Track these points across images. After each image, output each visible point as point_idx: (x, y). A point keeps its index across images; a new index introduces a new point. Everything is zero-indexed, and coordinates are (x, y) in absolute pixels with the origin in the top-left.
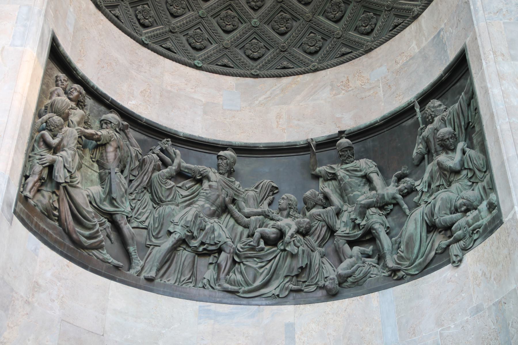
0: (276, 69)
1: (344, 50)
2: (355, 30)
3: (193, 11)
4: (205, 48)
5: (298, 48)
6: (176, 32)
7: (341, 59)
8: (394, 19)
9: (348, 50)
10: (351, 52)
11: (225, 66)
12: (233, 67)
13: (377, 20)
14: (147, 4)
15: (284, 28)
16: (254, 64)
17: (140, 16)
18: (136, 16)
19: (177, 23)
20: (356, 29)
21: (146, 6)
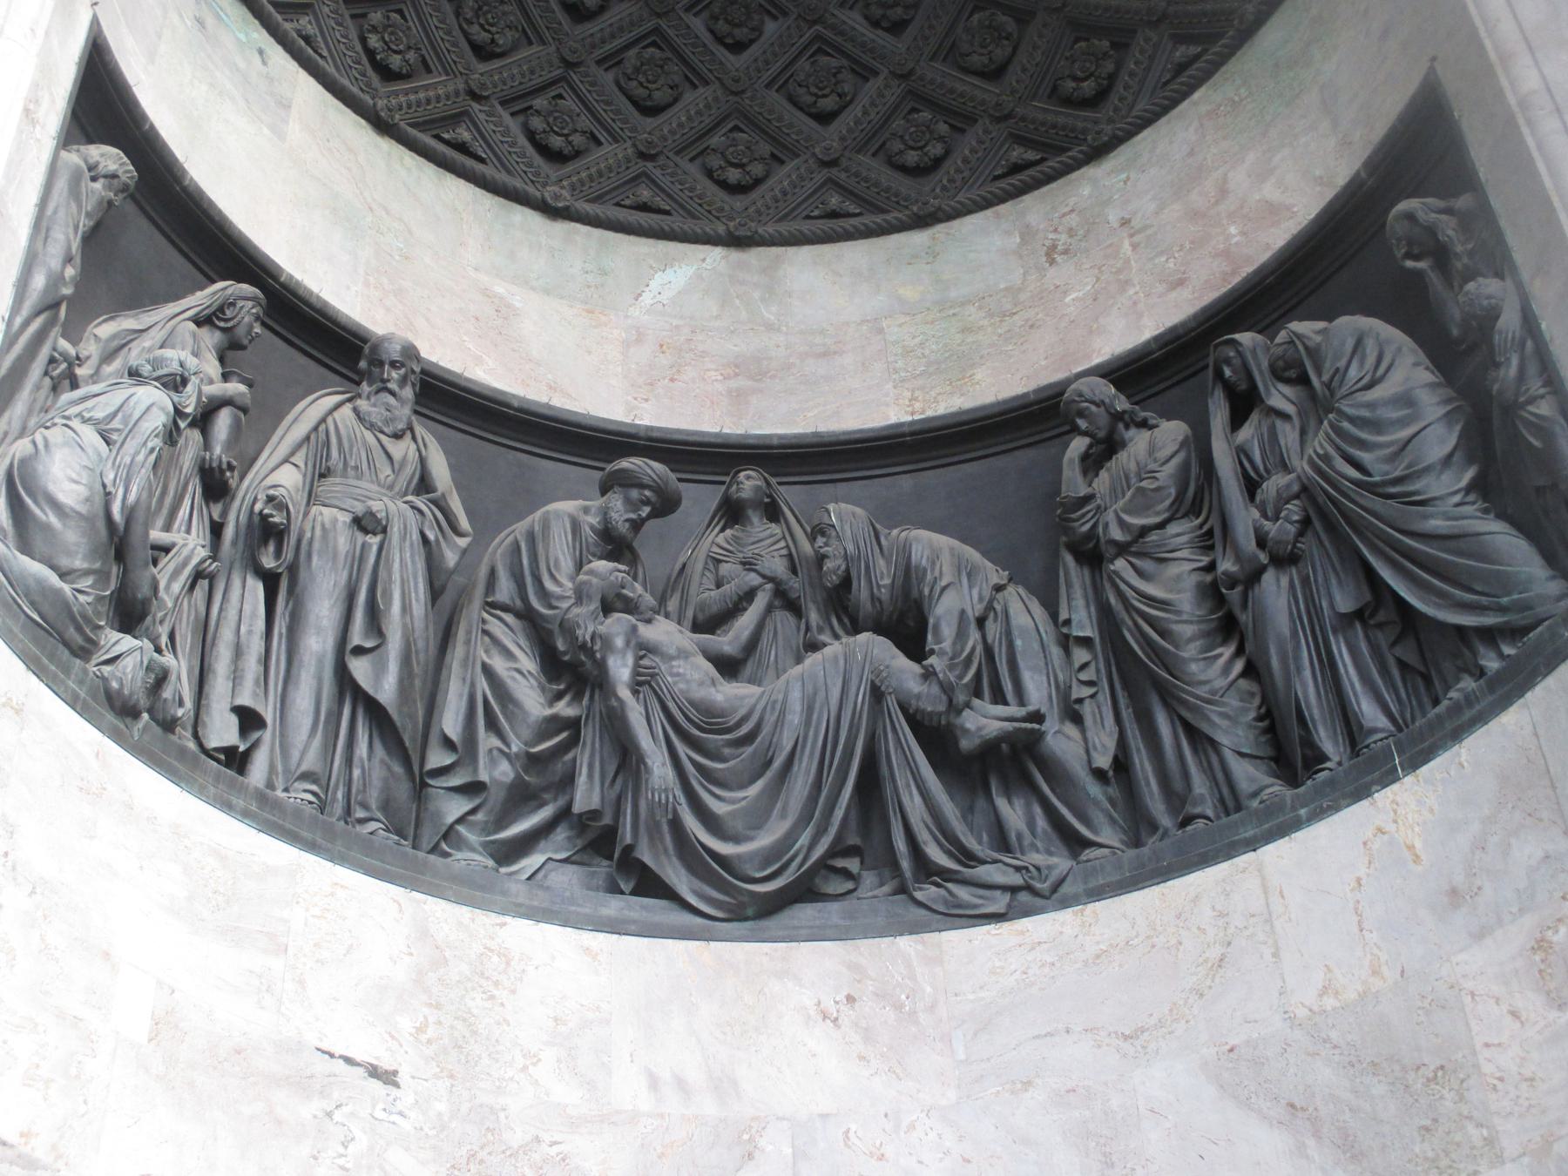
0: (808, 217)
1: (1017, 154)
2: (1049, 97)
3: (544, 43)
4: (577, 154)
5: (874, 155)
6: (486, 98)
7: (1015, 180)
9: (1032, 155)
10: (1043, 160)
12: (667, 213)
13: (1119, 65)
14: (400, 12)
15: (834, 97)
16: (738, 202)
17: (374, 41)
18: (363, 40)
19: (490, 73)
21: (394, 15)
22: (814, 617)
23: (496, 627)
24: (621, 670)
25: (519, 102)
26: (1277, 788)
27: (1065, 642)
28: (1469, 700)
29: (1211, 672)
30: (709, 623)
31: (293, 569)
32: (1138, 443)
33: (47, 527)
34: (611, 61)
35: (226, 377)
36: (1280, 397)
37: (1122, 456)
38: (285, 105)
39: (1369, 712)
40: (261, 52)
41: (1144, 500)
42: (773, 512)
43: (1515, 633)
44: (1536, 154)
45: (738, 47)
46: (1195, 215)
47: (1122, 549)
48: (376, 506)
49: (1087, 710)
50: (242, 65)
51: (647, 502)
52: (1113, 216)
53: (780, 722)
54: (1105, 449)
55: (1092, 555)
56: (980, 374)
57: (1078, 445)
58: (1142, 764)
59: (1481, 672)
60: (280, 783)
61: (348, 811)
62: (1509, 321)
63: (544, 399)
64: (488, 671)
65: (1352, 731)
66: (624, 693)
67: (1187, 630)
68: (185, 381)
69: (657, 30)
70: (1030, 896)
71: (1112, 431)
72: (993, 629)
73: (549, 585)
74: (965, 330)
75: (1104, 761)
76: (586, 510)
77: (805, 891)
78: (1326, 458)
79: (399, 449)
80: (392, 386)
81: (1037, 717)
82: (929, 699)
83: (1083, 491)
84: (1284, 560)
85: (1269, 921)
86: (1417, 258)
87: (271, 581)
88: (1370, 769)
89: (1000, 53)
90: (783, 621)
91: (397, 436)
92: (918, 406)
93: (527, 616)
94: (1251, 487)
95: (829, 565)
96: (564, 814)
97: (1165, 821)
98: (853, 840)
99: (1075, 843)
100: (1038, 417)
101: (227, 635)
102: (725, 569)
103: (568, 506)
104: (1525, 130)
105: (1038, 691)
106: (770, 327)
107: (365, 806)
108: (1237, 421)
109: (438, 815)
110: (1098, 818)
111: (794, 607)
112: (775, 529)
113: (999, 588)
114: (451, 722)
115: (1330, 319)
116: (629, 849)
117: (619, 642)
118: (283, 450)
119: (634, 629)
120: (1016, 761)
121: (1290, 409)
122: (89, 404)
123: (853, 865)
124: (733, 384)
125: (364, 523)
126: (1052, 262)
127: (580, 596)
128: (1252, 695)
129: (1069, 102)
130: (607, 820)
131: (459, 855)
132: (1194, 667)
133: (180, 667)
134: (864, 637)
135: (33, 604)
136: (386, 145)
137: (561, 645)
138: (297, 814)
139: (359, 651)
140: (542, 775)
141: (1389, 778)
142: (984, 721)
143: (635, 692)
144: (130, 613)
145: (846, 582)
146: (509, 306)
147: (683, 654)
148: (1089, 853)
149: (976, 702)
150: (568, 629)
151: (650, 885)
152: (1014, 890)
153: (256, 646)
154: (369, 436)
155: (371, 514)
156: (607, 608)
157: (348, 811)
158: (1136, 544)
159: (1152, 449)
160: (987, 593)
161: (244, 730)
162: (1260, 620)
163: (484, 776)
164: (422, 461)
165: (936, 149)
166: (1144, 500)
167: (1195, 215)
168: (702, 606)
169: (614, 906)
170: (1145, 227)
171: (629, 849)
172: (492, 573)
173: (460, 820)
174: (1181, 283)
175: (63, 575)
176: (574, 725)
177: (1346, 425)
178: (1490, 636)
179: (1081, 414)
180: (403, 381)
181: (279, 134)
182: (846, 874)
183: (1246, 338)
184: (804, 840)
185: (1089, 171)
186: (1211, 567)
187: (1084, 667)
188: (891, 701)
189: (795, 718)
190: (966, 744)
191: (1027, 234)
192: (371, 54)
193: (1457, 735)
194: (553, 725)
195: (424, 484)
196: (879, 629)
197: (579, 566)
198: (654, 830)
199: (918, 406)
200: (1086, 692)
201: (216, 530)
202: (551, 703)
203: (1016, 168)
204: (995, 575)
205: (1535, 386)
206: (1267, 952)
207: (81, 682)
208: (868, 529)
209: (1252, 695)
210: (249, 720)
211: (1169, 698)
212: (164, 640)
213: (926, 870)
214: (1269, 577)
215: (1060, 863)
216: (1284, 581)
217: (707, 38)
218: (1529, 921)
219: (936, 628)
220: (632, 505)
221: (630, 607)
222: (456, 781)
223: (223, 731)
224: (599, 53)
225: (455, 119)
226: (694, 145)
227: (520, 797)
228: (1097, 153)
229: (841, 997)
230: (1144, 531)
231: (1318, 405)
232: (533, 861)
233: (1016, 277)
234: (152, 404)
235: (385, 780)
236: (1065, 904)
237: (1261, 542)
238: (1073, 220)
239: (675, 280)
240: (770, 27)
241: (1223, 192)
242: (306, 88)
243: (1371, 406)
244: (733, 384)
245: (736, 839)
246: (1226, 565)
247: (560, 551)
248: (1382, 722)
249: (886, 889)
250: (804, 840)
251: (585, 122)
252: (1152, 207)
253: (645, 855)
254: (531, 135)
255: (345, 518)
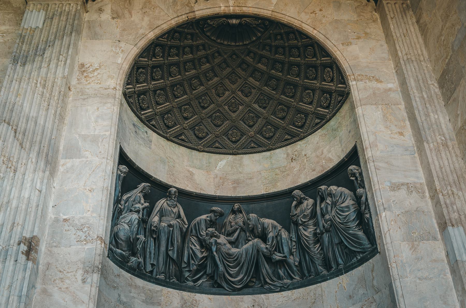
4: (204, 137)
8: (316, 120)
9: (289, 137)
10: (292, 138)
11: (217, 148)
13: (306, 120)
20: (294, 125)
22: (248, 234)
23: (193, 240)
24: (214, 249)
25: (192, 128)
26: (325, 272)
27: (291, 240)
28: (355, 263)
29: (315, 249)
30: (229, 235)
31: (158, 237)
32: (305, 202)
33: (121, 244)
34: (210, 117)
35: (145, 202)
36: (329, 200)
37: (302, 205)
38: (151, 142)
39: (340, 260)
40: (146, 132)
41: (305, 216)
42: (241, 212)
43: (363, 253)
44: (369, 170)
45: (234, 112)
46: (317, 157)
47: (301, 225)
48: (171, 223)
49: (294, 253)
50: (143, 136)
51: (218, 215)
52: (303, 153)
53: (241, 257)
54: (300, 203)
55: (296, 224)
56: (278, 184)
57: (294, 203)
58: (304, 264)
59: (357, 258)
60: (158, 274)
61: (169, 277)
62: (363, 198)
63: (199, 192)
64: (191, 248)
65: (338, 264)
66: (215, 253)
67: (311, 242)
68: (140, 211)
69: (219, 110)
70: (283, 289)
71: (301, 200)
72: (279, 238)
73: (201, 233)
74: (276, 174)
75: (297, 264)
76: (207, 217)
77: (246, 286)
78: (334, 216)
79: (175, 210)
80: (173, 198)
81: (285, 257)
82: (268, 254)
83: (295, 213)
84: (327, 231)
85: (322, 296)
86: (353, 177)
87: (155, 239)
88: (338, 273)
89: (284, 114)
90: (243, 234)
91: (174, 208)
92: (267, 190)
93: (197, 237)
94: (323, 215)
95: (250, 226)
96: (205, 273)
97: (307, 275)
98: (254, 276)
99: (292, 278)
100: (288, 193)
101: (148, 250)
102: (232, 224)
103: (204, 217)
104: (368, 164)
105: (286, 249)
106: (240, 173)
107: (172, 277)
108: (321, 202)
109: (184, 275)
110: (296, 273)
111: (244, 231)
112: (241, 215)
113: (280, 230)
114: (185, 259)
115: (339, 186)
116: (216, 280)
117: (214, 244)
118: (155, 213)
119: (216, 240)
120: (283, 263)
121: (330, 203)
122: (125, 219)
123: (254, 280)
124: (234, 185)
125: (170, 226)
126: (292, 161)
127: (207, 234)
128: (322, 254)
129: (296, 127)
130: (212, 275)
131: (188, 282)
132: (312, 249)
133: (141, 260)
134: (256, 240)
135: (120, 258)
136: (169, 143)
137: (204, 244)
138: (162, 280)
139: (170, 250)
140: (202, 267)
141: (342, 274)
142: (277, 256)
143: (216, 252)
144: (134, 254)
145: (253, 229)
146: (192, 173)
147: (225, 244)
148: (294, 281)
149: (275, 252)
150: (205, 241)
151: (220, 286)
152: (281, 287)
153: (153, 252)
154: (169, 208)
155: (170, 224)
156: (211, 237)
157: (169, 277)
158: (303, 224)
159: (307, 205)
160: (278, 231)
161: (152, 267)
162: (323, 241)
163: (192, 269)
164: (179, 211)
165: (271, 134)
166: (305, 216)
167: (317, 157)
168: (228, 231)
169: (214, 290)
170: (309, 157)
171: (216, 280)
172: (192, 229)
173: (188, 276)
174: (314, 170)
175: (124, 251)
176: (206, 257)
177: (337, 210)
178: (359, 252)
179: (295, 197)
180: (175, 198)
181: (150, 148)
182: (253, 282)
183: (323, 187)
184: (245, 278)
185: (299, 143)
186: (316, 229)
187: (294, 246)
188: (261, 253)
189: (244, 256)
190: (273, 261)
191: (288, 155)
192: (165, 124)
193: (352, 269)
194: (203, 257)
195: (179, 217)
196: (259, 237)
197: (207, 229)
198: (220, 278)
199: (267, 190)
200: (295, 250)
201: (145, 229)
202: (202, 254)
203: (286, 140)
204: (279, 227)
205: (367, 211)
206: (321, 302)
207: (127, 267)
208: (257, 219)
209: (322, 254)
210: (153, 265)
211: (308, 253)
212: (139, 255)
213: (266, 283)
214: (325, 234)
215: (288, 281)
216: (327, 235)
217: (228, 110)
218: (360, 304)
219: (268, 240)
220: (216, 216)
221: (216, 236)
222: (187, 269)
223: (149, 268)
224: (208, 116)
225: (181, 135)
226: (226, 133)
227: (197, 272)
228: (301, 139)
229: (252, 305)
230: (305, 222)
231: (334, 204)
232: (200, 282)
233: (286, 164)
234: (135, 216)
235: (175, 271)
236: (289, 290)
237: (324, 227)
238: (296, 153)
239: (223, 162)
240: (240, 107)
241: (322, 153)
242: (154, 136)
243: (342, 207)
244: (234, 185)
245: (235, 278)
246: (318, 231)
247: (203, 226)
248: (342, 263)
249: (260, 285)
250: (245, 278)
251: (206, 130)
252: (310, 153)
253: (219, 281)
254: (195, 134)
255: (166, 225)
